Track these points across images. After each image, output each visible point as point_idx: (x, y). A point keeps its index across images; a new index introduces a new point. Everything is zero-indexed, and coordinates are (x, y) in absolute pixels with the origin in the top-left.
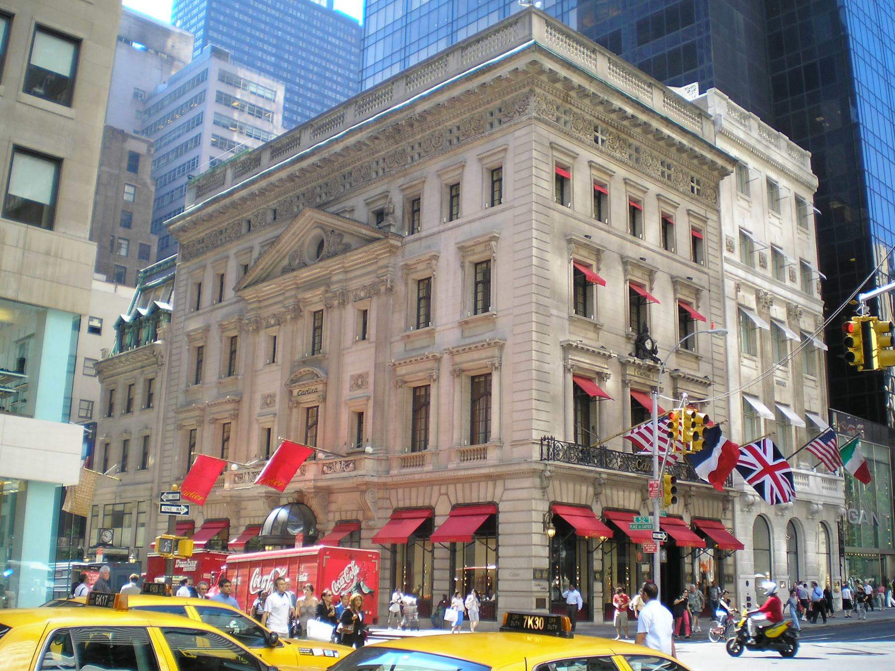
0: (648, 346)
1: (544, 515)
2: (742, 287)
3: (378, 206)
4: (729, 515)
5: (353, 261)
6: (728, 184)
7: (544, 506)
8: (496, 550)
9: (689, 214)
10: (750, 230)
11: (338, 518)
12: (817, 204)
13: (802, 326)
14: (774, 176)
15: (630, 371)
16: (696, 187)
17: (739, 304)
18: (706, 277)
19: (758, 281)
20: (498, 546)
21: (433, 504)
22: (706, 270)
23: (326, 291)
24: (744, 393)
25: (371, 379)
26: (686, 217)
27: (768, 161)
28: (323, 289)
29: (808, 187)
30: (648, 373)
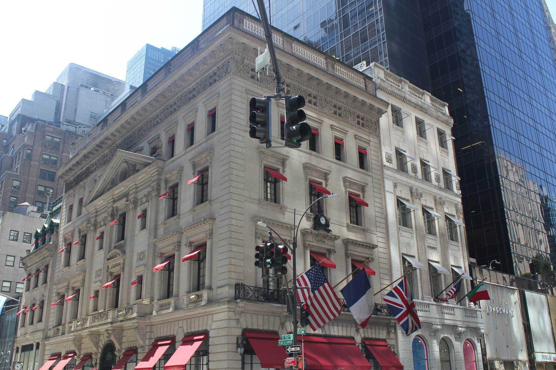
0: (323, 221)
1: (237, 338)
2: (398, 185)
3: (153, 145)
4: (392, 336)
5: (140, 180)
6: (386, 120)
7: (239, 332)
8: (207, 364)
9: (356, 138)
10: (405, 150)
11: (126, 346)
12: (453, 134)
13: (446, 210)
14: (421, 116)
15: (310, 238)
16: (361, 121)
17: (397, 196)
18: (371, 178)
19: (412, 182)
20: (208, 361)
21: (175, 334)
22: (370, 174)
23: (127, 201)
24: (403, 254)
25: (146, 254)
26: (354, 140)
27: (416, 106)
28: (125, 199)
29: (447, 123)
30: (324, 240)
